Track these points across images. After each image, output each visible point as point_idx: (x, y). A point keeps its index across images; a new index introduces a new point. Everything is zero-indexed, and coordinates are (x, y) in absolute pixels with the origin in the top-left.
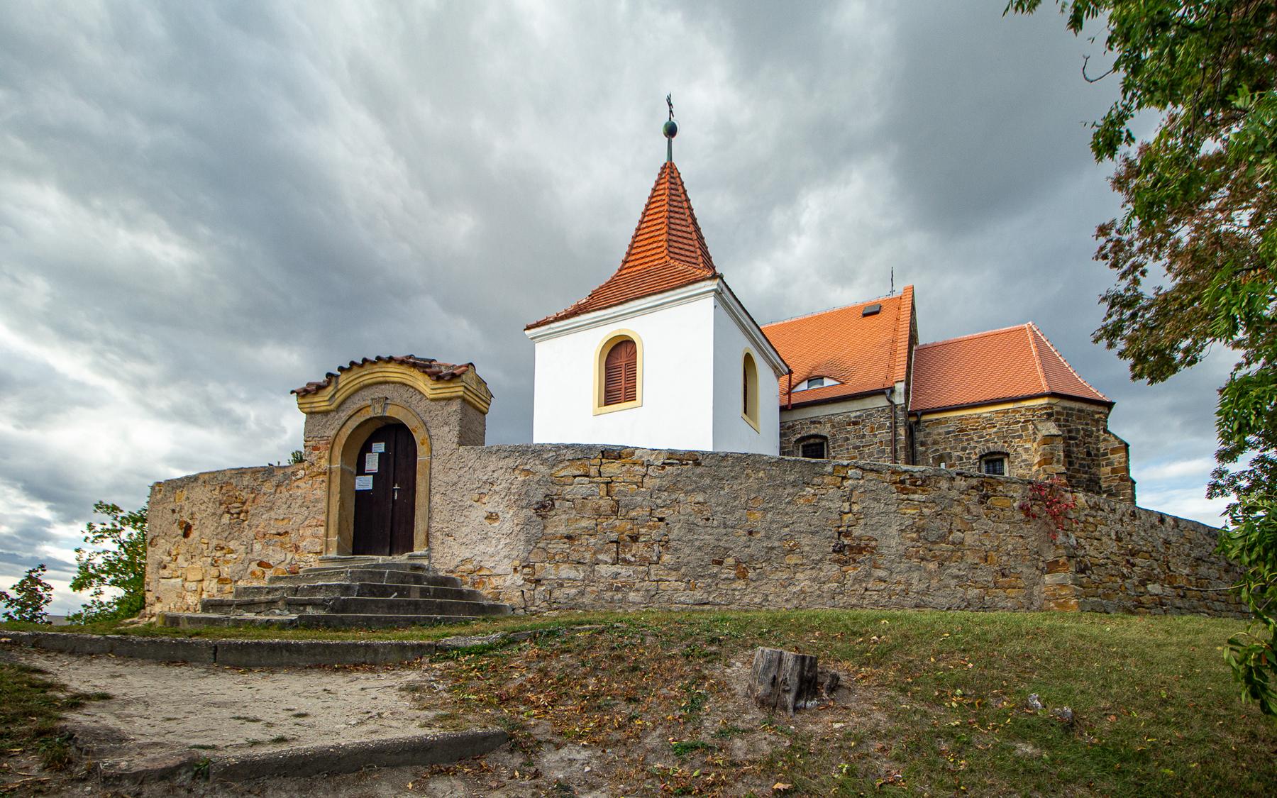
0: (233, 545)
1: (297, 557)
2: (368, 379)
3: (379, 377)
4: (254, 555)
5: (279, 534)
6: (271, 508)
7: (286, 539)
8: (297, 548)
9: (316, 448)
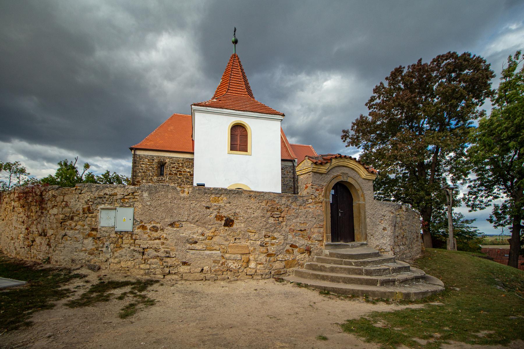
0: (276, 235)
1: (310, 242)
2: (341, 164)
3: (345, 164)
4: (289, 241)
5: (301, 230)
6: (297, 217)
7: (305, 233)
8: (310, 238)
9: (317, 190)
